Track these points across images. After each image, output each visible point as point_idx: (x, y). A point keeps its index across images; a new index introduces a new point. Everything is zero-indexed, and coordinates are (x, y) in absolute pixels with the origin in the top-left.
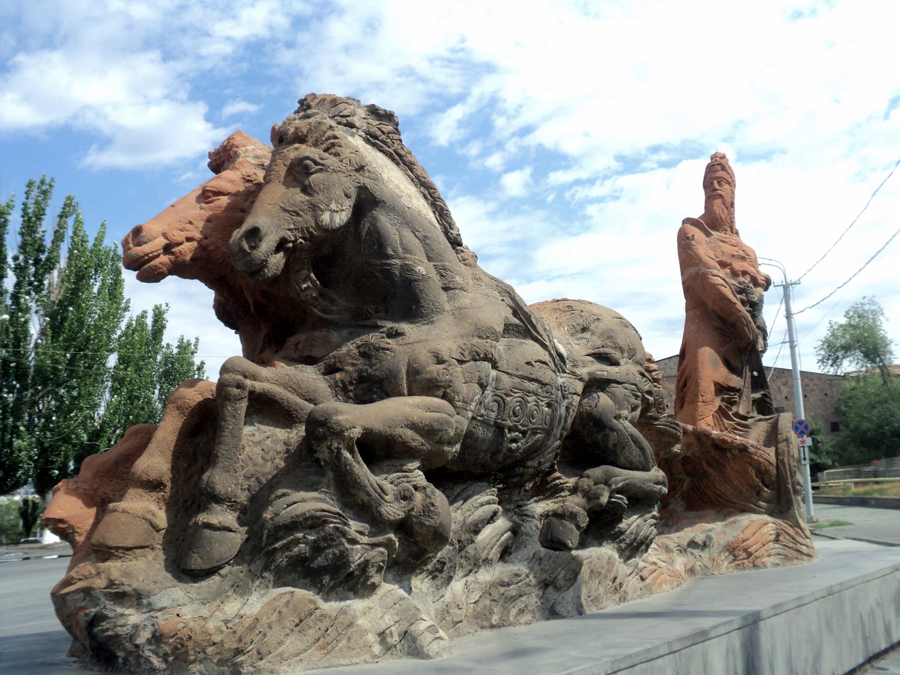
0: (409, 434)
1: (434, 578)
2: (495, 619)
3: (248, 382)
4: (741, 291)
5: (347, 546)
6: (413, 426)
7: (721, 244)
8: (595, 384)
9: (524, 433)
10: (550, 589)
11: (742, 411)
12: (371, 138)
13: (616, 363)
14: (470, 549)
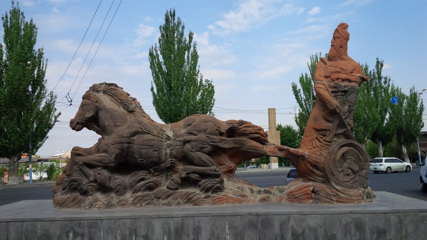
0: (95, 162)
1: (116, 193)
2: (138, 205)
3: (75, 152)
4: (335, 87)
5: (83, 186)
6: (95, 161)
7: (329, 68)
8: (185, 142)
9: (145, 159)
10: (160, 199)
11: (328, 139)
12: (105, 92)
13: (195, 135)
14: (135, 187)
